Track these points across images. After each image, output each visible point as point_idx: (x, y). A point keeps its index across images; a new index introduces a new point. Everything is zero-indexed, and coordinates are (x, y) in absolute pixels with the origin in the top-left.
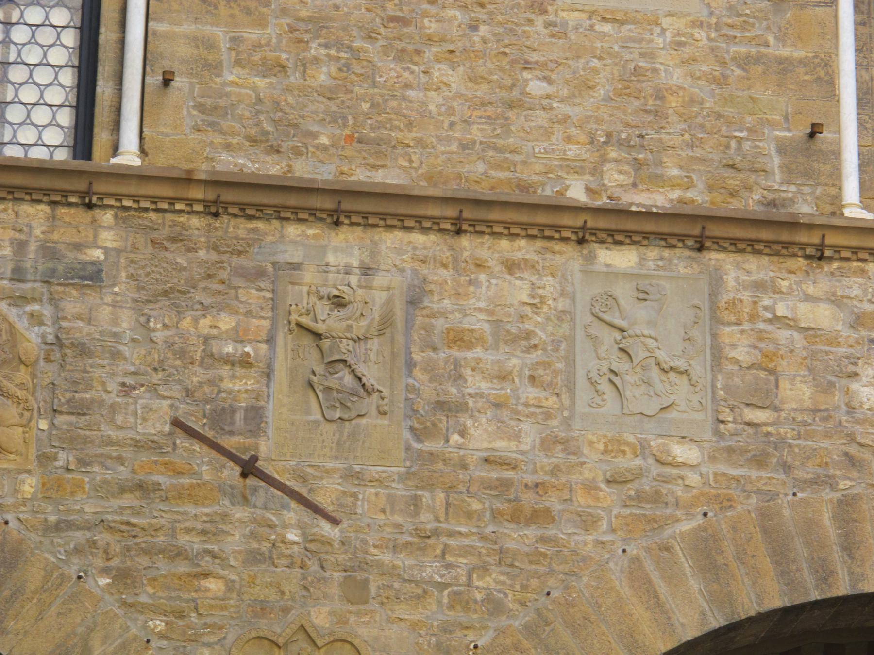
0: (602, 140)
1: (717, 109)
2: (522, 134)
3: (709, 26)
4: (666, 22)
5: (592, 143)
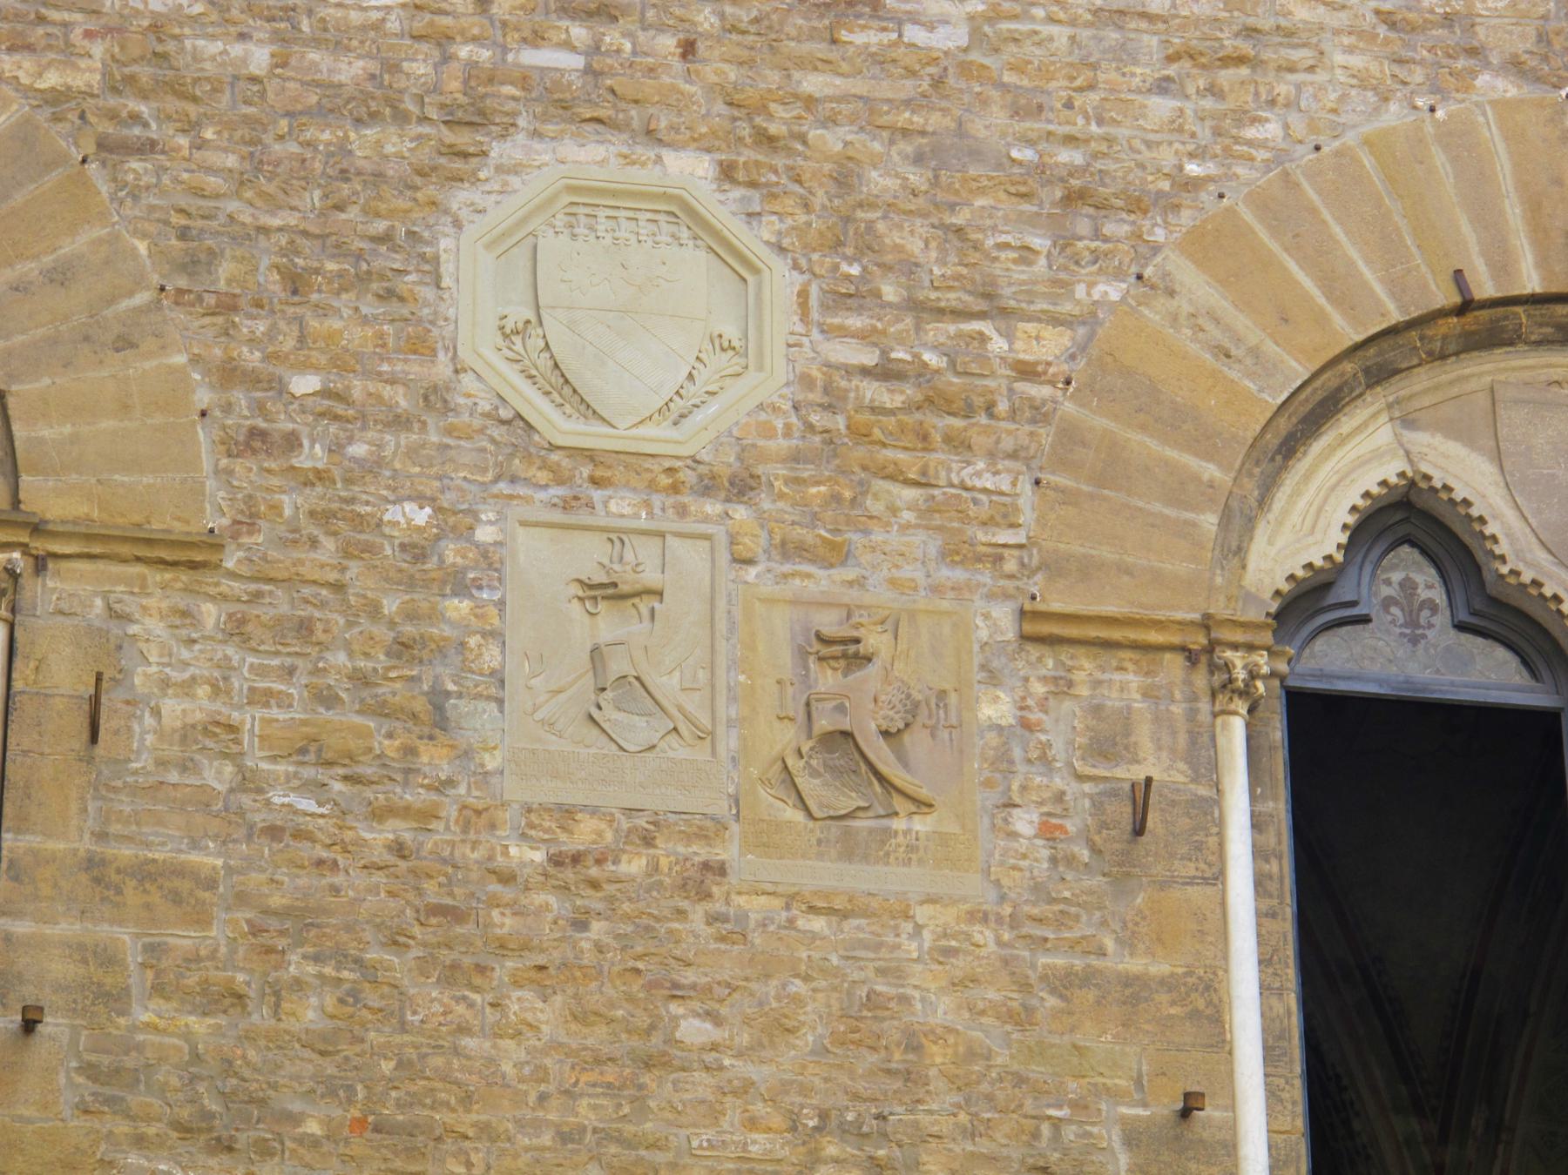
0: (811, 1124)
1: (1015, 1067)
2: (670, 1116)
3: (999, 920)
4: (922, 913)
5: (794, 1129)
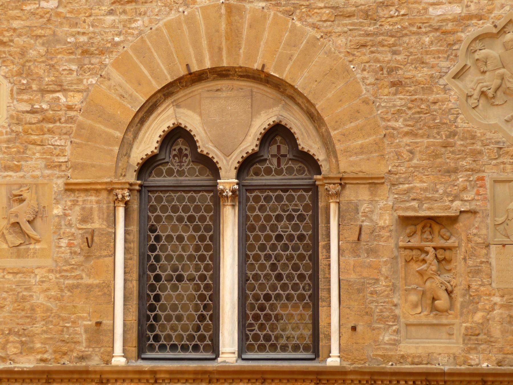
0: (7, 332)
4: (37, 271)
5: (2, 334)
